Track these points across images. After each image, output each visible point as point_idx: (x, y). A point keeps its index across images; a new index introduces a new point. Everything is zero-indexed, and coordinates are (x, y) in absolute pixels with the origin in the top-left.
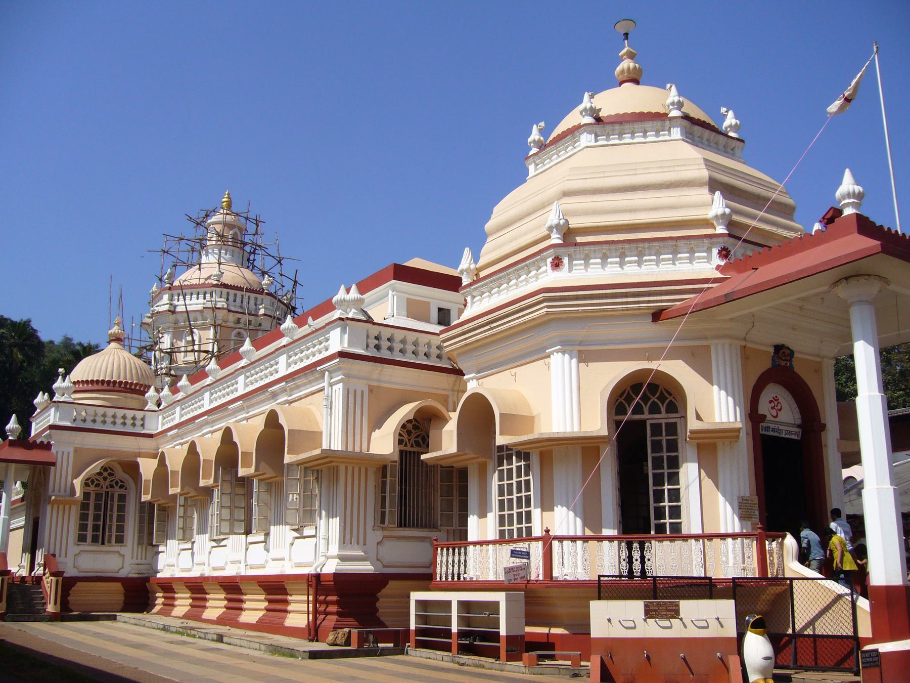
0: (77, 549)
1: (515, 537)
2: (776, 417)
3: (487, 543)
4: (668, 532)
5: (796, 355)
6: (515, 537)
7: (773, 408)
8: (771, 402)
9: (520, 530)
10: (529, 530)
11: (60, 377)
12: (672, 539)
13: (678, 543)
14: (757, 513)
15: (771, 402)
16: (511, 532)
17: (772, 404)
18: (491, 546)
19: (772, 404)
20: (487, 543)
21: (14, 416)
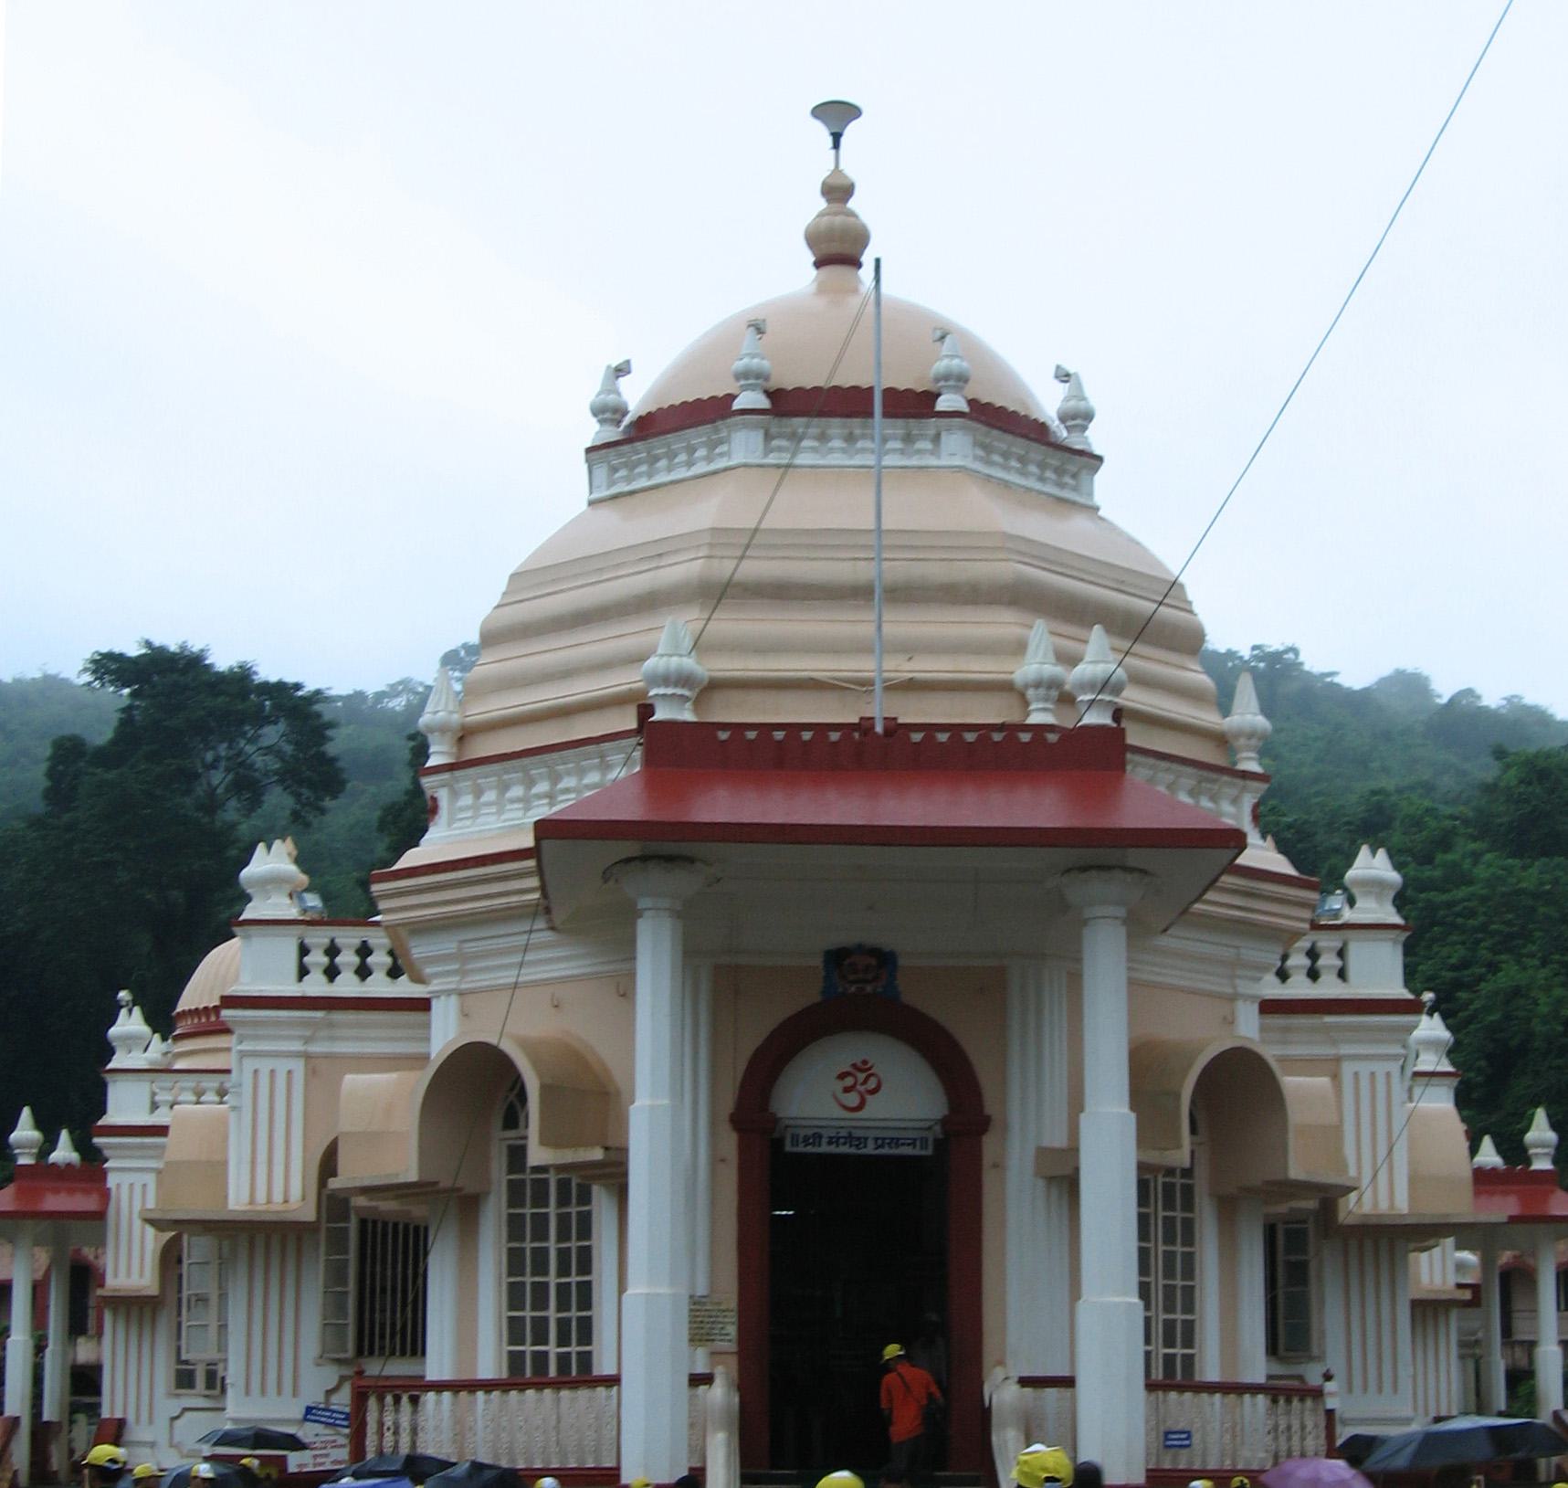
0: (174, 1406)
1: (553, 1372)
2: (859, 1108)
3: (473, 1386)
4: (528, 1373)
5: (902, 962)
6: (553, 1372)
7: (847, 1090)
8: (842, 1076)
9: (564, 1360)
10: (586, 1359)
11: (123, 1012)
12: (574, 1384)
13: (583, 1394)
14: (732, 1330)
15: (842, 1076)
16: (541, 1359)
17: (849, 1081)
18: (447, 1395)
19: (849, 1081)
20: (473, 1386)
21: (26, 1112)
